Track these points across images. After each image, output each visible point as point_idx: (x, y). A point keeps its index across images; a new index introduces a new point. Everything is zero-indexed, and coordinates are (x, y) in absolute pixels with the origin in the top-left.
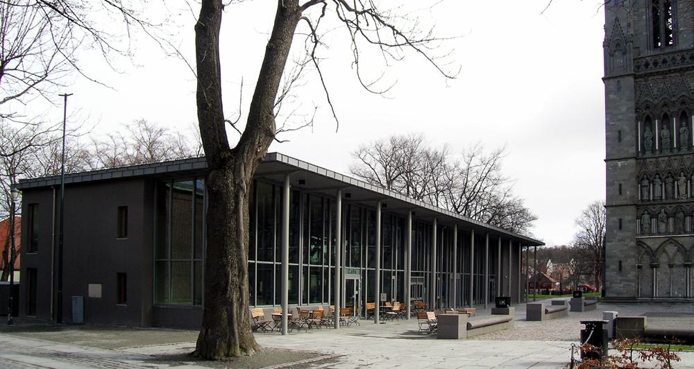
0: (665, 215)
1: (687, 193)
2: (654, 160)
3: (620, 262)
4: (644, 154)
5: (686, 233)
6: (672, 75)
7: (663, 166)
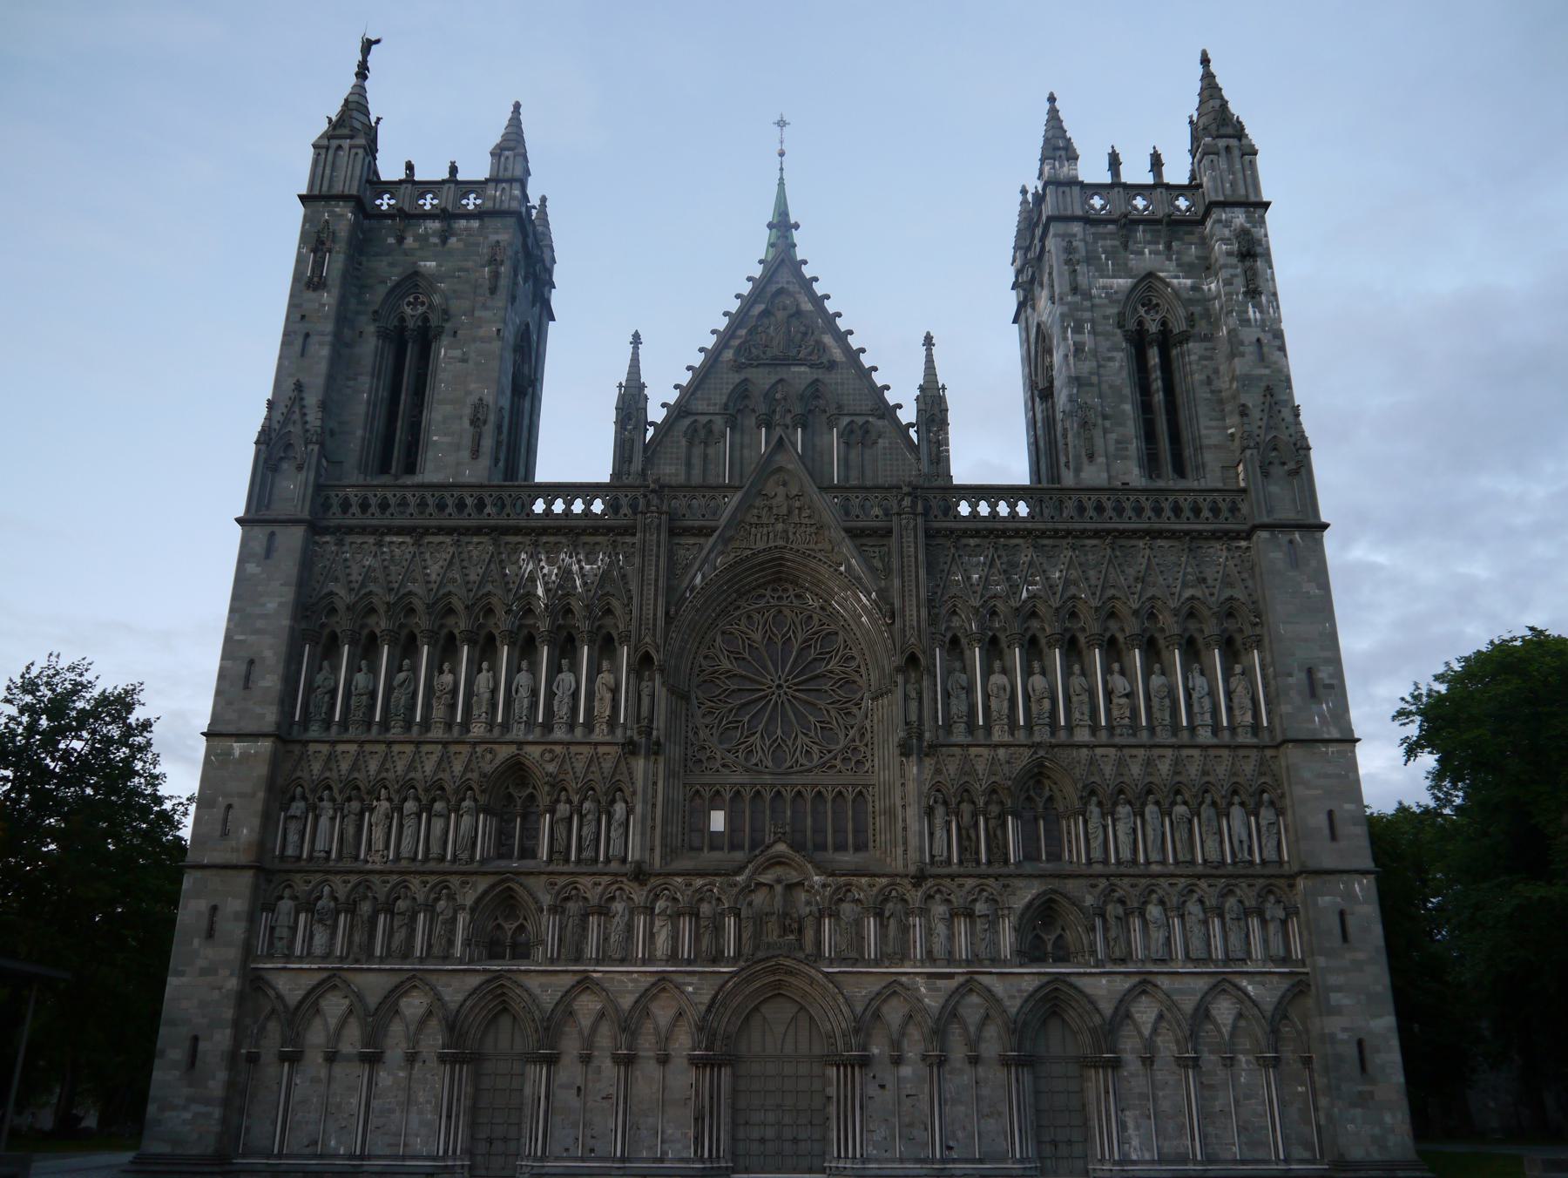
0: (332, 904)
1: (387, 847)
2: (325, 749)
3: (195, 1039)
4: (306, 729)
5: (370, 956)
6: (395, 539)
7: (345, 766)
